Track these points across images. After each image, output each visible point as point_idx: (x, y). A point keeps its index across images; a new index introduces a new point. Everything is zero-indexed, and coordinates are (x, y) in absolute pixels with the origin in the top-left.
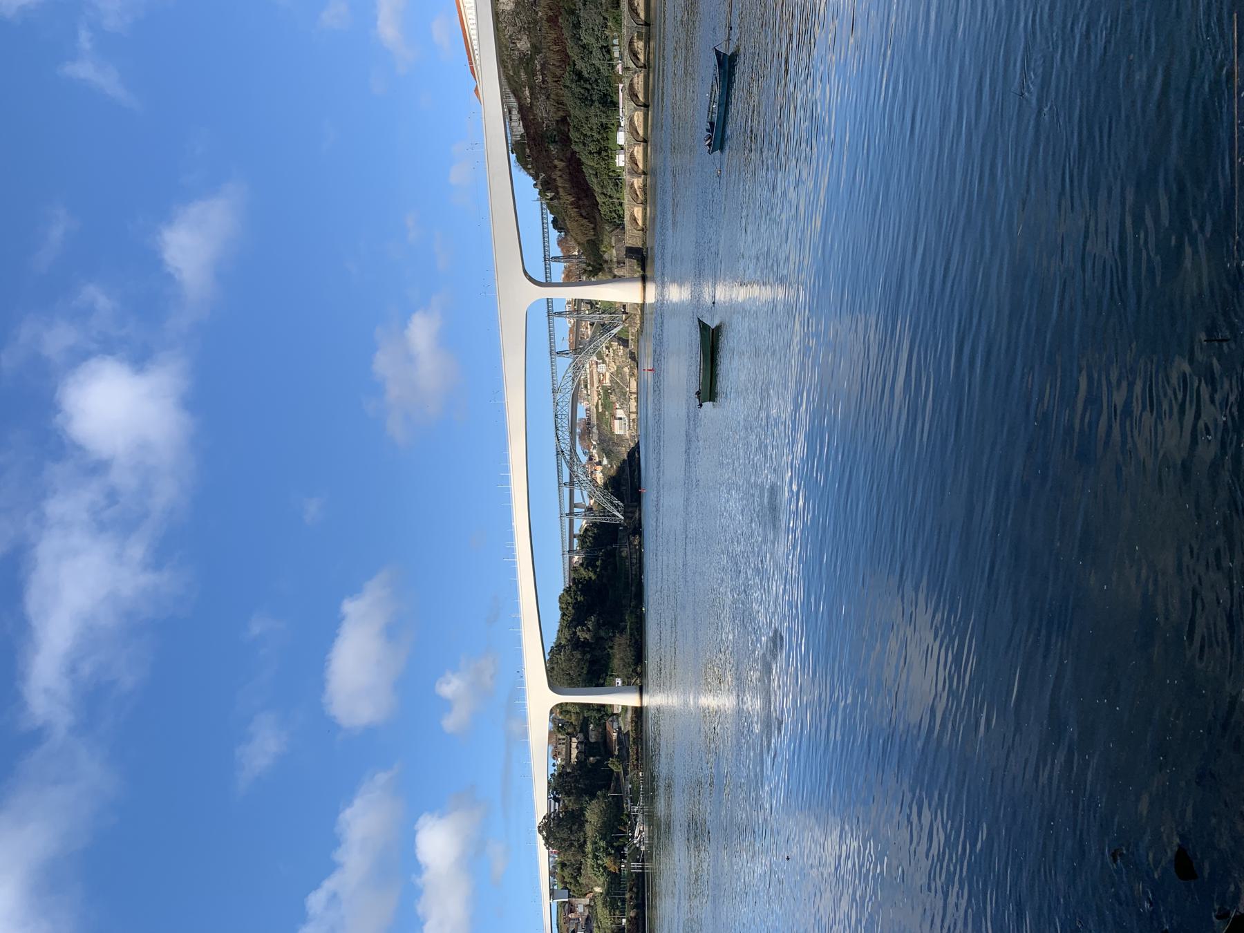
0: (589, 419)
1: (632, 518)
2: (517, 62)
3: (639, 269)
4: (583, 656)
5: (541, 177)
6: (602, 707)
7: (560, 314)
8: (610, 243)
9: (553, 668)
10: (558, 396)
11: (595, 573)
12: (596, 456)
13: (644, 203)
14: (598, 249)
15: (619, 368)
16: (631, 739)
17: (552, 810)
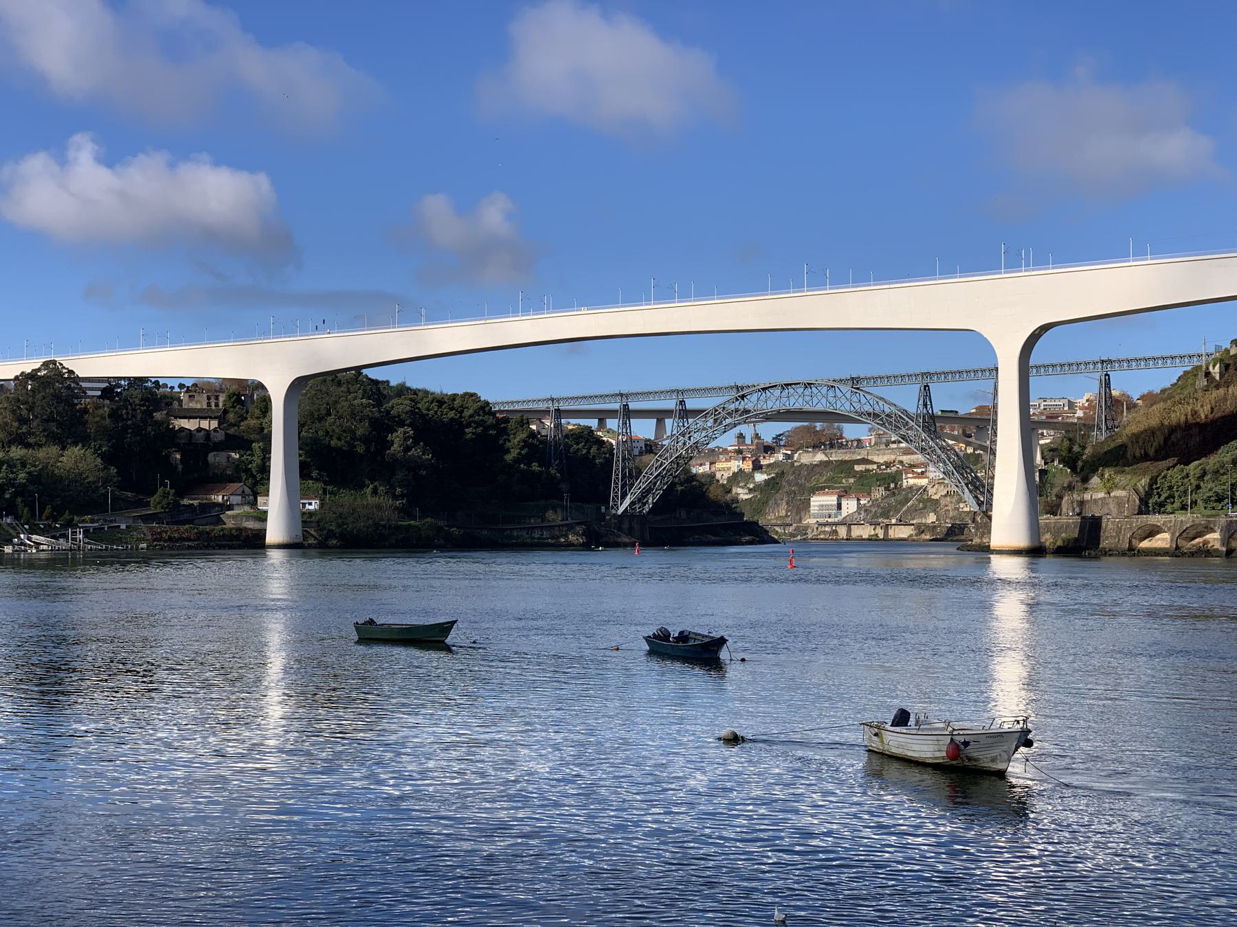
0: (841, 446)
1: (620, 529)
3: (1059, 543)
4: (360, 440)
8: (1116, 487)
9: (339, 384)
10: (846, 389)
11: (517, 460)
12: (772, 460)
13: (1175, 552)
14: (1106, 464)
15: (933, 505)
16: (208, 528)
17: (84, 385)
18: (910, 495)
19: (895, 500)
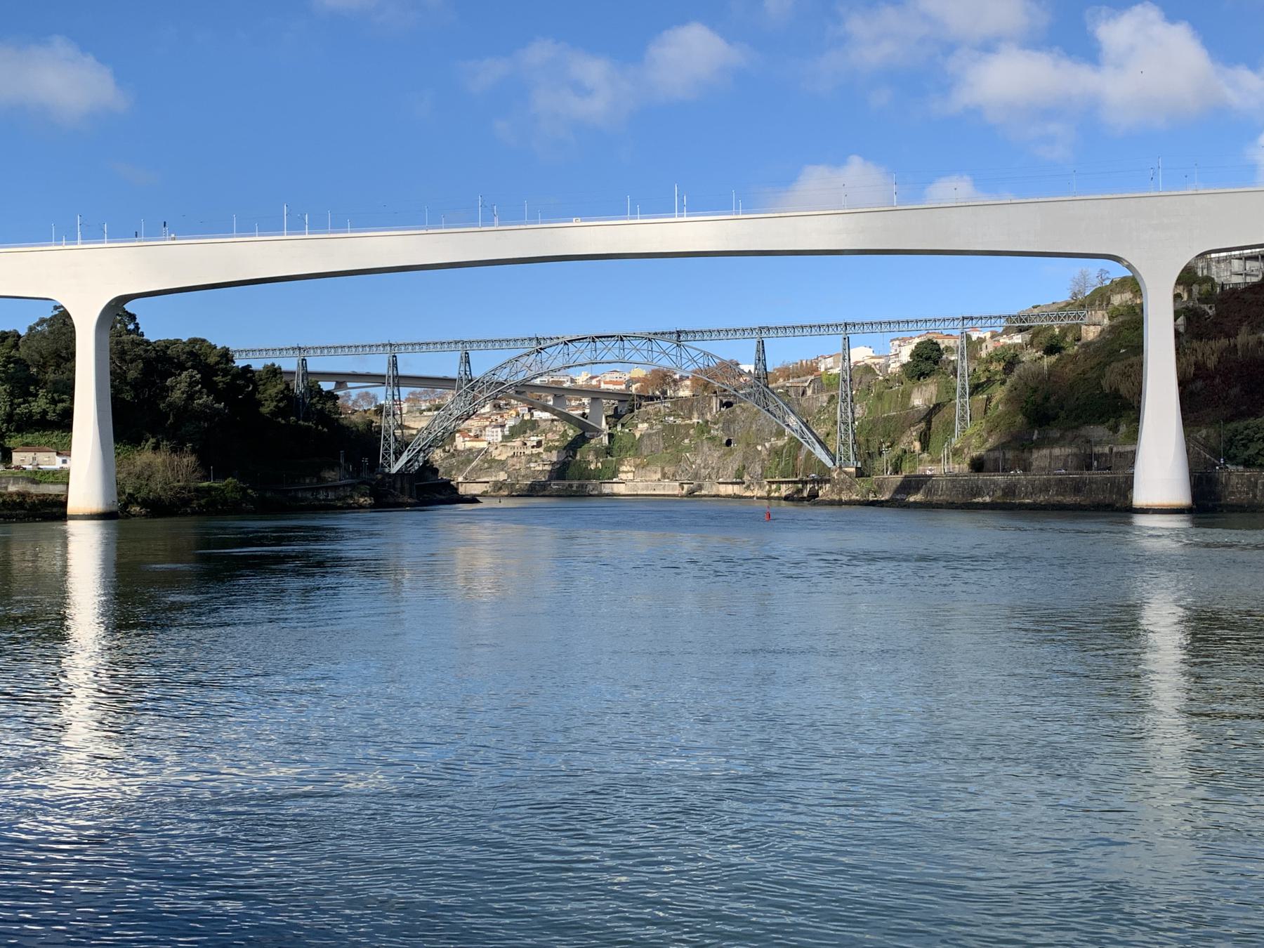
5: (1206, 307)
6: (64, 422)
11: (273, 413)
15: (502, 465)
18: (471, 456)
19: (458, 461)
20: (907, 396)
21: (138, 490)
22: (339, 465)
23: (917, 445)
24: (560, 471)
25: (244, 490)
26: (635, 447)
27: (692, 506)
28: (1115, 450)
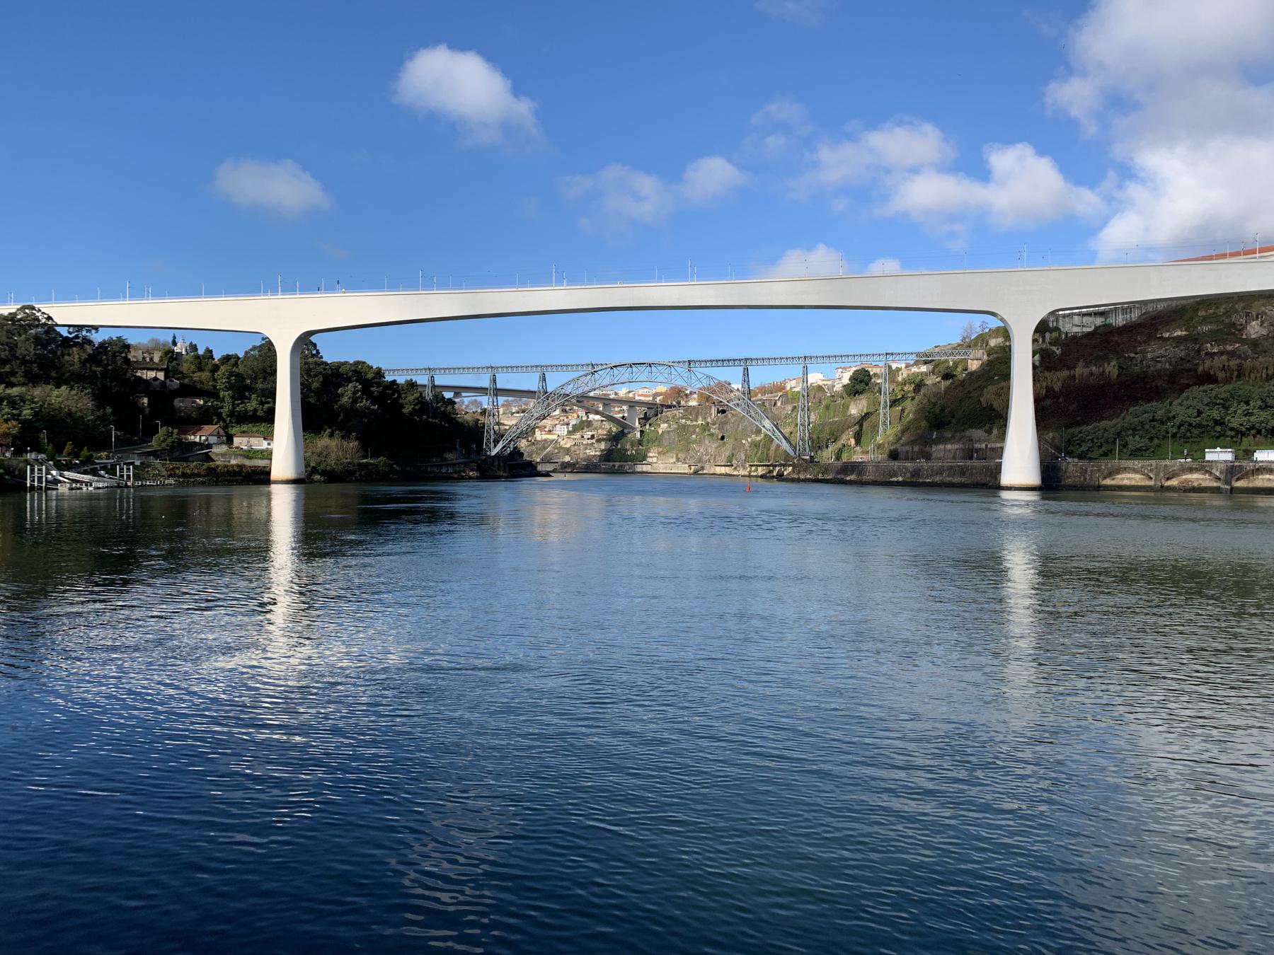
1: (494, 466)
2: (1227, 321)
5: (1054, 348)
6: (269, 417)
7: (746, 373)
11: (412, 413)
20: (846, 407)
21: (319, 464)
22: (456, 450)
23: (853, 441)
24: (607, 456)
25: (392, 465)
26: (658, 440)
27: (697, 481)
28: (989, 446)
